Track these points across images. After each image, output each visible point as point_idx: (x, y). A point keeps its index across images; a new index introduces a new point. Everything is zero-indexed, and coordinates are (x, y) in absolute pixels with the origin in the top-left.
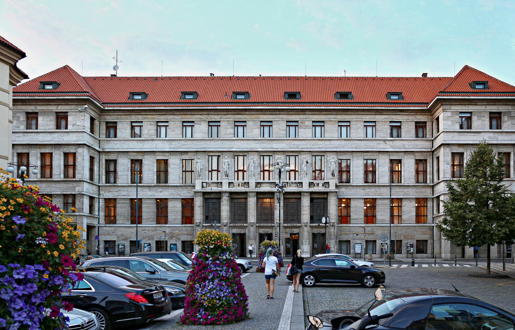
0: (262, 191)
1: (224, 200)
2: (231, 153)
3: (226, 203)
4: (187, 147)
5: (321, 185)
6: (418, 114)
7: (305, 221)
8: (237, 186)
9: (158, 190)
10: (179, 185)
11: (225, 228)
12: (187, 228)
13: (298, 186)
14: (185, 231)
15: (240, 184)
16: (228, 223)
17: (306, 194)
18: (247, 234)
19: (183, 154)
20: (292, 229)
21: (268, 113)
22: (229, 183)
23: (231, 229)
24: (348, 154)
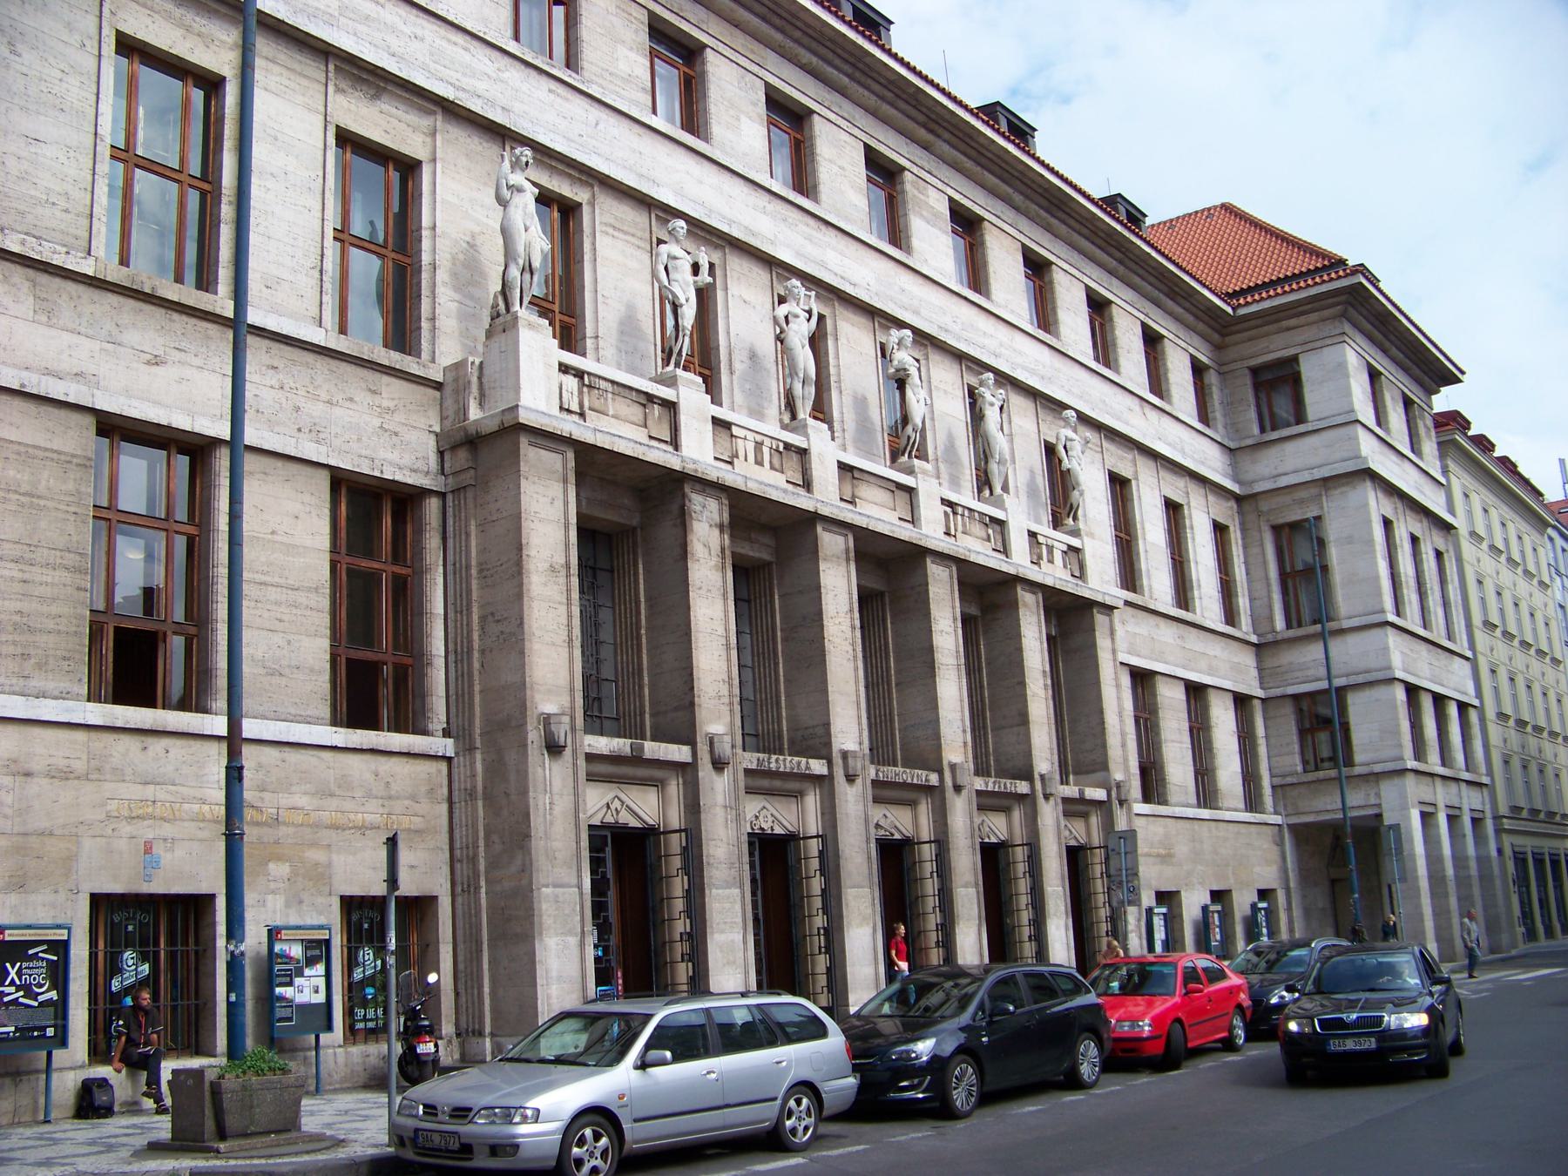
5: (1058, 556)
6: (1201, 326)
9: (132, 337)
14: (369, 795)
21: (806, 57)
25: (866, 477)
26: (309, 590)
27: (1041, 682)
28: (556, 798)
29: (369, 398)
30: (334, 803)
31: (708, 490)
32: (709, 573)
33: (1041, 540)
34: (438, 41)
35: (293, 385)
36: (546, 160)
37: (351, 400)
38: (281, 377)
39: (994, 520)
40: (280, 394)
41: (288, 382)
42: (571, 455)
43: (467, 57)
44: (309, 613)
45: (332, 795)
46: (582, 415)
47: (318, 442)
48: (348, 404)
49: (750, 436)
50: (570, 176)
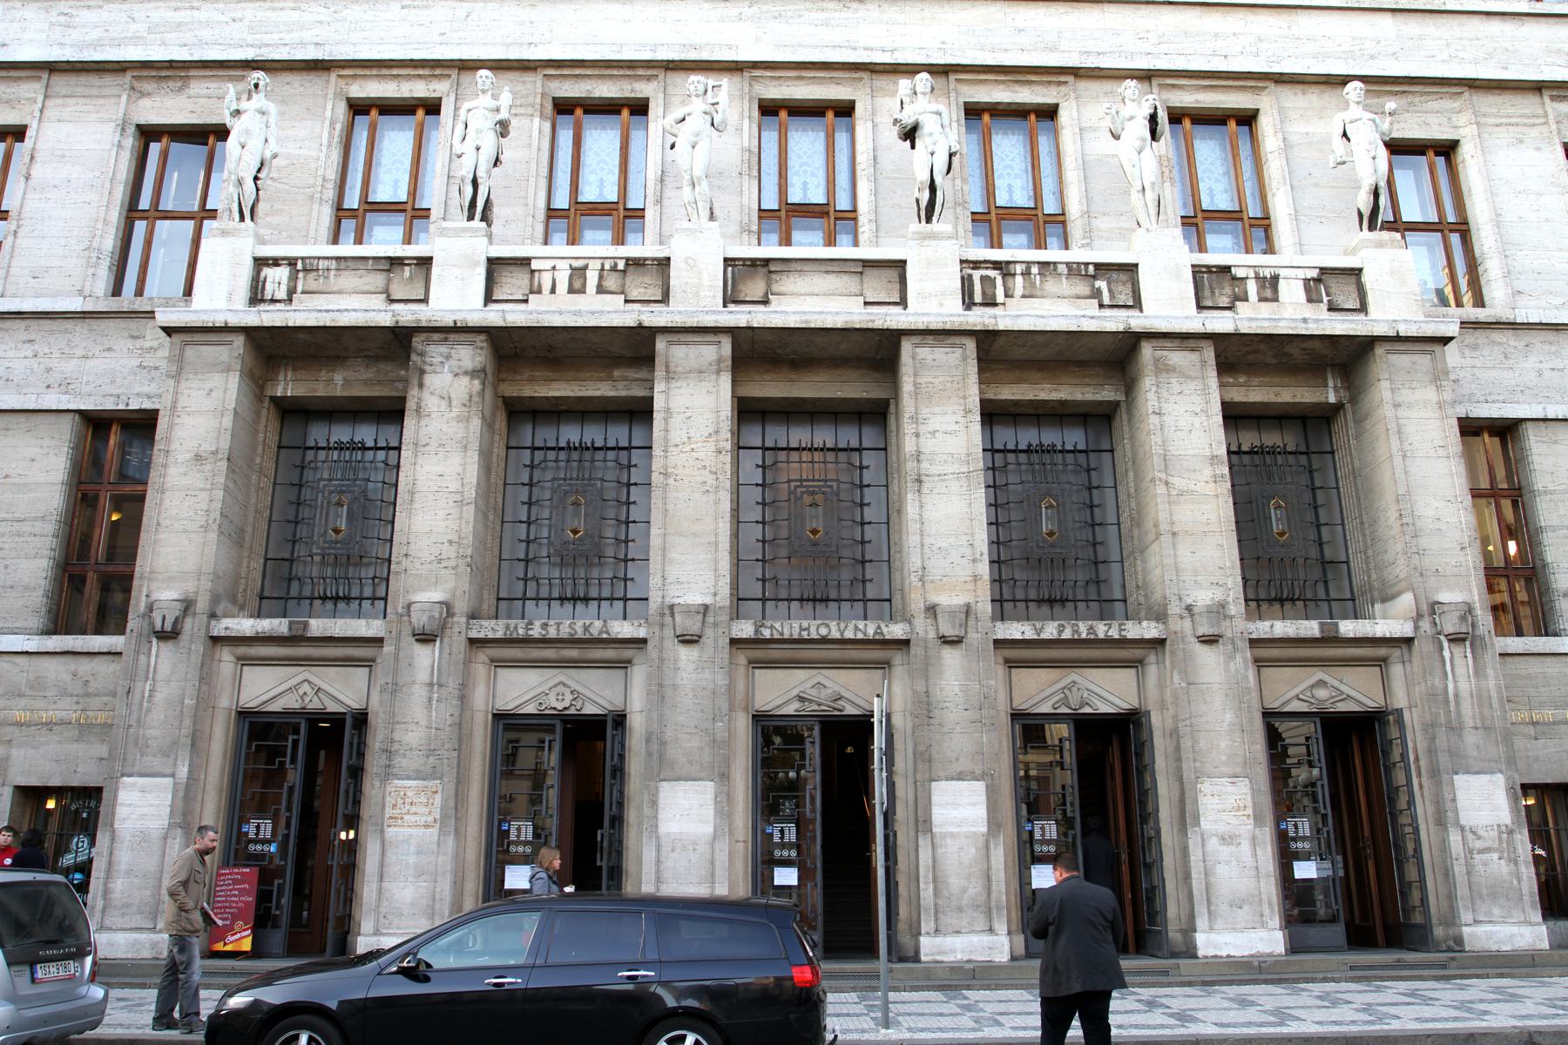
0: (792, 322)
1: (431, 403)
2: (529, 78)
3: (454, 430)
4: (188, 37)
5: (1292, 290)
7: (1203, 597)
8: (562, 287)
10: (76, 305)
11: (424, 659)
12: (85, 666)
13: (1097, 294)
14: (64, 693)
15: (592, 278)
16: (461, 606)
17: (1178, 357)
18: (637, 723)
19: (148, 86)
20: (1074, 676)
22: (494, 264)
23: (480, 669)
24: (1434, 105)
25: (794, 266)
26: (36, 519)
27: (1207, 472)
28: (159, 685)
29: (130, 344)
30: (23, 702)
31: (452, 337)
32: (444, 427)
33: (1240, 273)
34: (260, 15)
35: (47, 351)
36: (385, 72)
37: (109, 349)
38: (37, 347)
39: (1102, 268)
40: (34, 363)
41: (42, 348)
42: (239, 341)
43: (296, 15)
44: (32, 538)
45: (21, 695)
46: (290, 300)
47: (66, 393)
48: (106, 354)
49: (560, 264)
50: (420, 76)
